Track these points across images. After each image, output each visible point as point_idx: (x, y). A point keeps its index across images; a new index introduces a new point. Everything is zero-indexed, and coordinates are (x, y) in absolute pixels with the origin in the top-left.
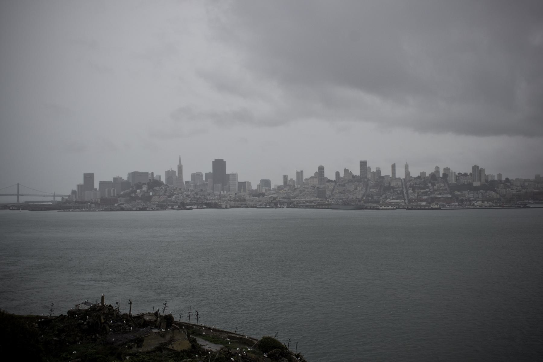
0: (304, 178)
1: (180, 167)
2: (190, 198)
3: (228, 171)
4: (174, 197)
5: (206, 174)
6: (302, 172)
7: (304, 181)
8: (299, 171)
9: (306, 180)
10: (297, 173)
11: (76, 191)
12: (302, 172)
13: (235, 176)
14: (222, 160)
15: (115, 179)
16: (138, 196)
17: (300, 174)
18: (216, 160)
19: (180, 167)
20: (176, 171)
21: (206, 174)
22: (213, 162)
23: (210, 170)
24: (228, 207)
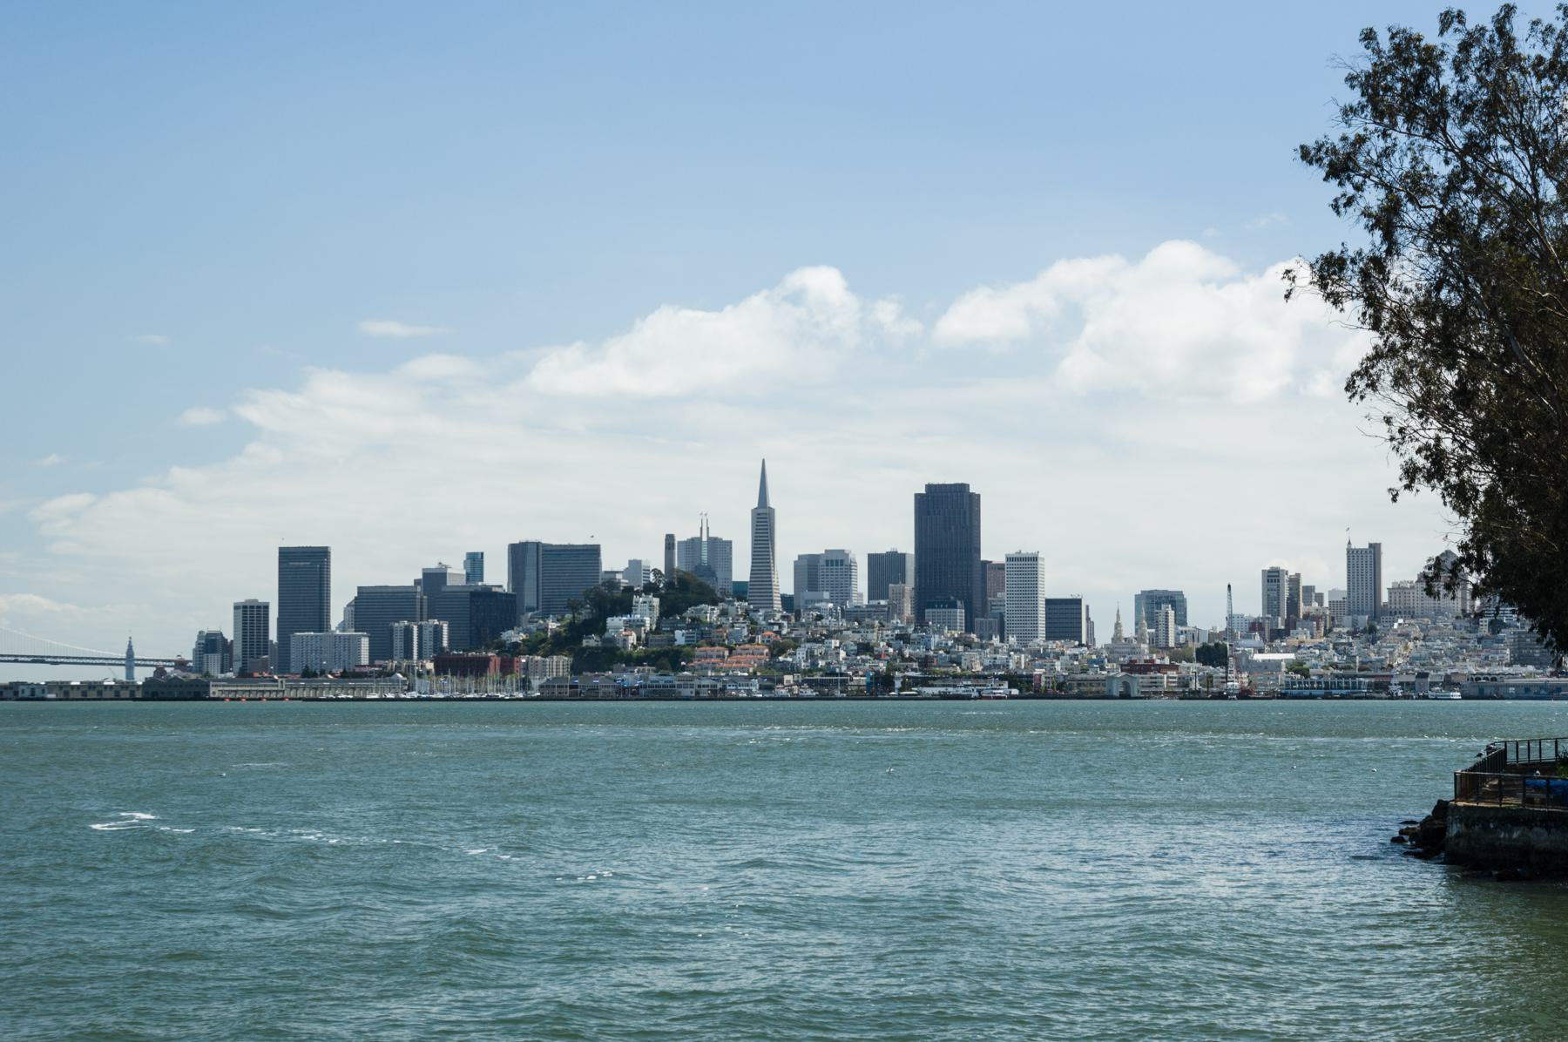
0: (1386, 583)
1: (763, 523)
2: (878, 657)
3: (994, 547)
4: (801, 653)
5: (874, 560)
6: (1375, 549)
7: (1385, 598)
8: (1361, 544)
9: (1397, 590)
10: (1353, 554)
11: (229, 635)
12: (1375, 549)
13: (1026, 566)
14: (962, 489)
15: (434, 579)
16: (618, 649)
17: (1365, 562)
18: (929, 487)
19: (763, 523)
20: (726, 547)
21: (874, 560)
22: (918, 497)
23: (902, 538)
24: (1135, 693)
